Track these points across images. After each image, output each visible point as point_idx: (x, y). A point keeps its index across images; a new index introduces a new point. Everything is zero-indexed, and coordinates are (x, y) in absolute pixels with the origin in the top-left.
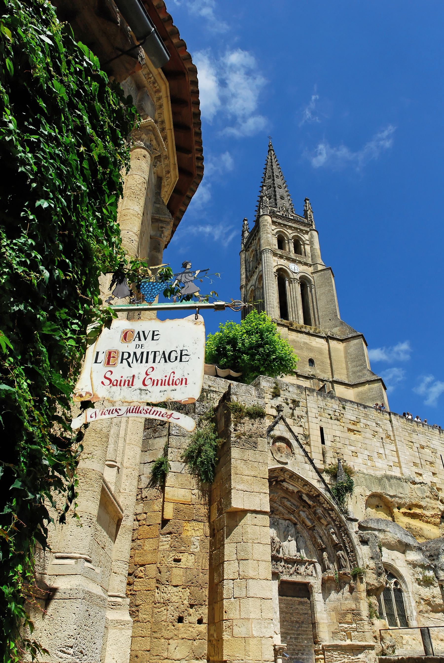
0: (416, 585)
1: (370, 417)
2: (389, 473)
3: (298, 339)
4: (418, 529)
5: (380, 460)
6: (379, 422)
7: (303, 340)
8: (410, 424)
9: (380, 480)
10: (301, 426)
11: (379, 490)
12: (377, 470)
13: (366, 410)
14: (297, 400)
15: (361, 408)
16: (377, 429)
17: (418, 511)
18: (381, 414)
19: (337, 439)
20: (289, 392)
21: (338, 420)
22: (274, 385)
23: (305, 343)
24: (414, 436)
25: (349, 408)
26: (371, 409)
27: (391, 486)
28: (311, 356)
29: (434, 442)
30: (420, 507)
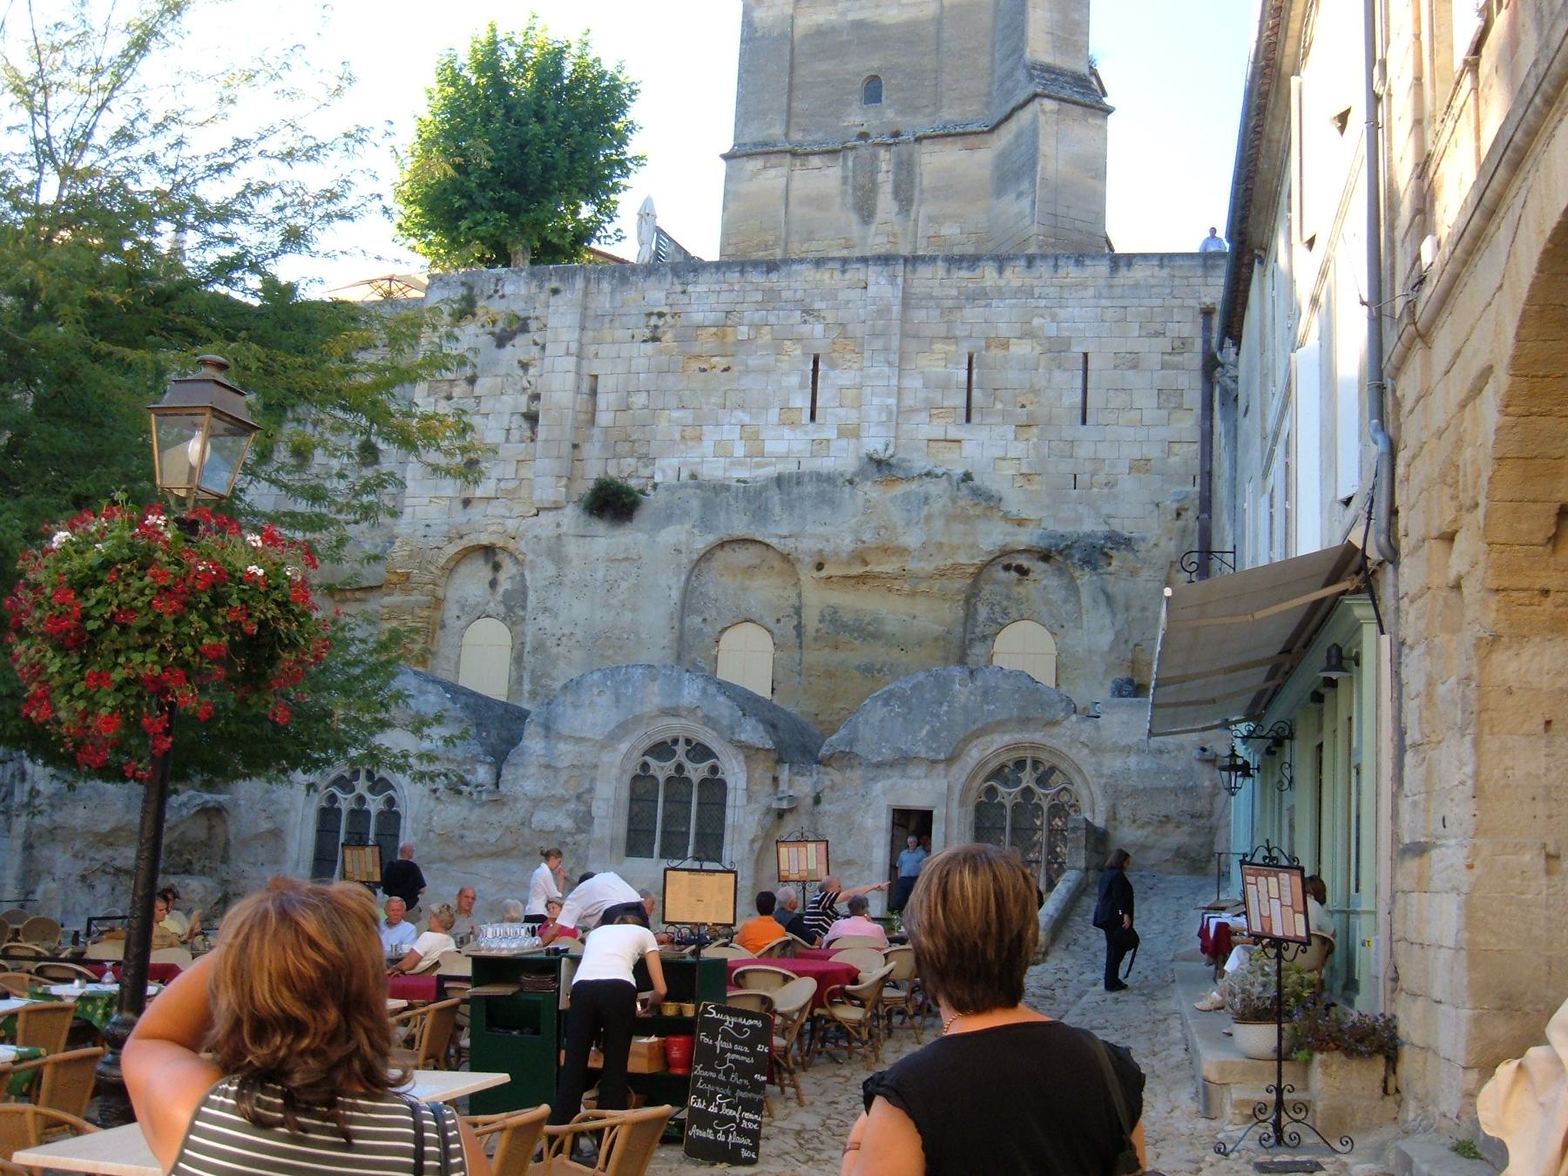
0: (432, 803)
1: (785, 295)
2: (809, 465)
3: (833, 17)
4: (868, 619)
5: (787, 432)
6: (817, 305)
7: (851, 17)
8: (964, 274)
9: (754, 497)
10: (524, 389)
11: (740, 526)
12: (758, 466)
13: (774, 276)
14: (522, 314)
15: (756, 277)
16: (806, 329)
17: (889, 566)
18: (837, 275)
19: (640, 400)
20: (503, 296)
21: (655, 339)
22: (462, 291)
23: (859, 25)
24: (972, 314)
25: (701, 288)
26: (795, 267)
27: (789, 506)
28: (873, 63)
29: (1062, 314)
30: (902, 551)
